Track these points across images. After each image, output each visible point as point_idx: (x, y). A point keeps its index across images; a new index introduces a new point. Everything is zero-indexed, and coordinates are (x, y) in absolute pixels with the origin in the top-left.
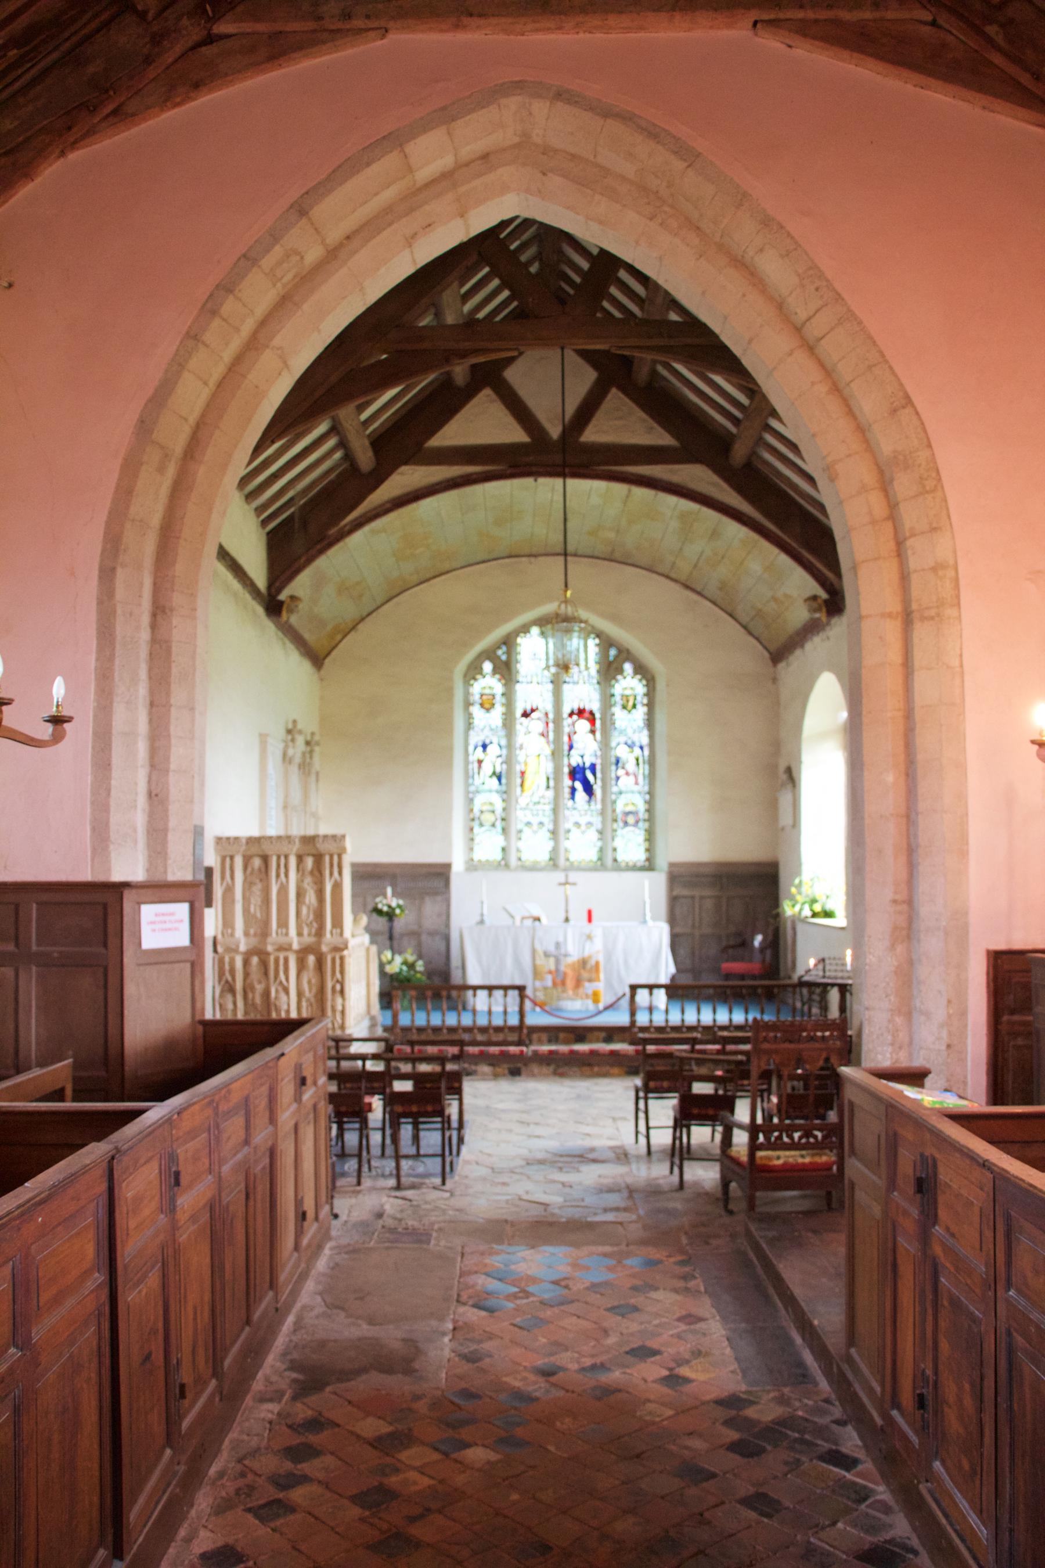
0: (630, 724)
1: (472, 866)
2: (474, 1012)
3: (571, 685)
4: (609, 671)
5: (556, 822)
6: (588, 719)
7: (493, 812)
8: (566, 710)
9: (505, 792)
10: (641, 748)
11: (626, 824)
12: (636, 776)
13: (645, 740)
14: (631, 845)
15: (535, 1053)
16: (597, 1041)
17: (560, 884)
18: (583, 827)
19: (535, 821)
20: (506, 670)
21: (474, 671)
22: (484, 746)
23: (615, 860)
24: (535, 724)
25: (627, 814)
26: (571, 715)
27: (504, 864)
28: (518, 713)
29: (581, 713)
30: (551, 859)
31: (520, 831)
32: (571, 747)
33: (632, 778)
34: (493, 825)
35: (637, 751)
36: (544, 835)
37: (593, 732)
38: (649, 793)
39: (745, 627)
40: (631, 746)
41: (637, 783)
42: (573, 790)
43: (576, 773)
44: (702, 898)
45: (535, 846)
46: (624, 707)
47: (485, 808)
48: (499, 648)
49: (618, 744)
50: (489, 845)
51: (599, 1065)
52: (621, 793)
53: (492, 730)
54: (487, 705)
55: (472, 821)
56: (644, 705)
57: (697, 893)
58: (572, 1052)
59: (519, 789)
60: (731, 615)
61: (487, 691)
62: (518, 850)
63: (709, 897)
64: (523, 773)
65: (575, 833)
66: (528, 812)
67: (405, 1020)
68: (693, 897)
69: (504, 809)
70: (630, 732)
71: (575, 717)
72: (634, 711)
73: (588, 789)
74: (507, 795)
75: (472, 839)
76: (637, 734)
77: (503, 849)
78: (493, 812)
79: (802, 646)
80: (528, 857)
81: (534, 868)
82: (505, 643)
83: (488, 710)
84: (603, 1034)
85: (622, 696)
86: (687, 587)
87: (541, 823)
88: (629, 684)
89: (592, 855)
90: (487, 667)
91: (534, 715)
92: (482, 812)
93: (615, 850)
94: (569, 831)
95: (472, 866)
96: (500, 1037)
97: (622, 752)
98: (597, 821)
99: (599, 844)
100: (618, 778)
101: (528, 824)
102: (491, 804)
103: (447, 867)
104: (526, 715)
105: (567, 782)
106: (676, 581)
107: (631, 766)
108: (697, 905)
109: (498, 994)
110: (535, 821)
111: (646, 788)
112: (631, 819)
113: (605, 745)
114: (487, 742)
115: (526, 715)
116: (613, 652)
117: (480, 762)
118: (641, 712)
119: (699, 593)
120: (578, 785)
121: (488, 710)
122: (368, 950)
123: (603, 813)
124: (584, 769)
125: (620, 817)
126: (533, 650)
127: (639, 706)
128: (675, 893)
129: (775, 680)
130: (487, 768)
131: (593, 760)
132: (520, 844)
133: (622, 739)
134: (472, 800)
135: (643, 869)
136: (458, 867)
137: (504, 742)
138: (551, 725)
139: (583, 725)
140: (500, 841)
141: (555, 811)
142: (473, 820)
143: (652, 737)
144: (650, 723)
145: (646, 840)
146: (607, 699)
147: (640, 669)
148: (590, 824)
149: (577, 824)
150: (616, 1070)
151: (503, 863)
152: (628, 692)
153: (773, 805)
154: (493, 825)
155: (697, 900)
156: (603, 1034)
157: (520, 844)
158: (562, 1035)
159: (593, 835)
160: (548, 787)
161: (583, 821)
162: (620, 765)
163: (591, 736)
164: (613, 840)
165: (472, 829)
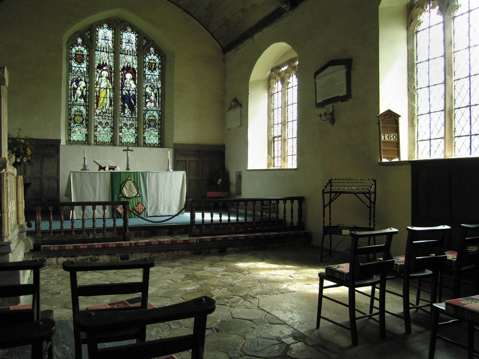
0: (153, 76)
1: (70, 142)
2: (72, 221)
3: (124, 56)
4: (141, 51)
5: (115, 122)
6: (131, 73)
7: (82, 116)
8: (121, 66)
9: (88, 106)
10: (158, 89)
11: (150, 126)
12: (155, 103)
13: (159, 86)
14: (152, 137)
15: (136, 245)
16: (164, 235)
17: (124, 150)
18: (129, 126)
19: (104, 122)
20: (91, 43)
21: (72, 43)
22: (77, 82)
23: (145, 143)
24: (105, 74)
25: (150, 121)
26: (124, 69)
27: (87, 142)
28: (96, 65)
29: (128, 69)
30: (111, 141)
31: (96, 127)
32: (123, 86)
33: (153, 104)
34: (82, 123)
35: (156, 90)
36: (108, 129)
37: (134, 79)
38: (160, 111)
39: (212, 34)
40: (153, 88)
41: (155, 106)
42: (124, 108)
43: (125, 99)
44: (190, 161)
45: (103, 134)
46: (150, 69)
47: (77, 114)
48: (86, 31)
49: (147, 86)
50: (78, 135)
51: (177, 250)
52: (148, 110)
53: (81, 73)
54: (79, 59)
55: (71, 120)
56: (159, 69)
57: (188, 159)
58: (159, 242)
59: (95, 105)
60: (205, 28)
61: (79, 53)
62: (95, 136)
63: (194, 161)
64: (98, 97)
65: (125, 129)
66: (100, 117)
67: (45, 226)
68: (186, 161)
69: (87, 115)
70: (152, 80)
71: (125, 71)
72: (154, 71)
73: (132, 108)
74: (88, 107)
75: (70, 130)
76: (156, 83)
77: (87, 135)
78: (82, 116)
79: (253, 37)
80: (100, 139)
81: (103, 144)
82: (89, 30)
83: (80, 63)
84: (167, 230)
85: (149, 63)
86: (185, 11)
87: (107, 123)
88: (152, 57)
89: (132, 140)
90: (80, 41)
91: (105, 68)
92: (75, 115)
93: (144, 138)
94: (121, 128)
95: (70, 142)
96: (100, 236)
97: (148, 90)
98: (135, 123)
99: (136, 135)
100: (147, 103)
101: (100, 123)
102: (80, 111)
103: (59, 141)
104: (100, 67)
105: (121, 103)
106: (180, 7)
107: (152, 98)
108: (188, 165)
109: (99, 208)
110: (104, 122)
111: (160, 109)
112: (152, 124)
113: (139, 87)
114: (79, 79)
115: (100, 67)
116: (145, 42)
117: (75, 89)
118: (157, 73)
119: (191, 15)
120: (126, 105)
121: (80, 63)
122: (17, 179)
123: (138, 119)
124: (130, 97)
125: (147, 121)
126: (105, 34)
127: (157, 69)
128: (177, 159)
129: (224, 61)
130: (79, 92)
131: (134, 93)
132: (96, 133)
133: (149, 84)
134: (70, 109)
135: (158, 147)
136: (63, 142)
137: (87, 80)
138: (113, 74)
139: (129, 76)
140: (84, 130)
141: (114, 117)
142: (70, 119)
143: (163, 84)
144: (162, 77)
145: (159, 134)
146: (141, 63)
147: (158, 52)
148: (131, 125)
149: (126, 125)
150: (188, 253)
151: (86, 143)
152: (152, 61)
153: (222, 119)
154: (82, 123)
155: (188, 162)
156: (167, 230)
157: (96, 133)
158: (143, 232)
159: (133, 131)
160: (111, 105)
161: (128, 123)
162: (147, 97)
163: (132, 82)
164: (144, 134)
165: (70, 124)
